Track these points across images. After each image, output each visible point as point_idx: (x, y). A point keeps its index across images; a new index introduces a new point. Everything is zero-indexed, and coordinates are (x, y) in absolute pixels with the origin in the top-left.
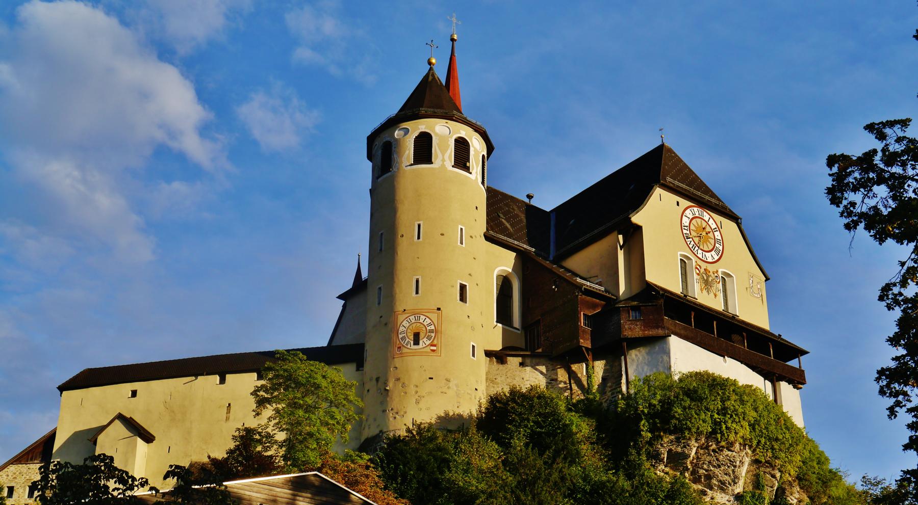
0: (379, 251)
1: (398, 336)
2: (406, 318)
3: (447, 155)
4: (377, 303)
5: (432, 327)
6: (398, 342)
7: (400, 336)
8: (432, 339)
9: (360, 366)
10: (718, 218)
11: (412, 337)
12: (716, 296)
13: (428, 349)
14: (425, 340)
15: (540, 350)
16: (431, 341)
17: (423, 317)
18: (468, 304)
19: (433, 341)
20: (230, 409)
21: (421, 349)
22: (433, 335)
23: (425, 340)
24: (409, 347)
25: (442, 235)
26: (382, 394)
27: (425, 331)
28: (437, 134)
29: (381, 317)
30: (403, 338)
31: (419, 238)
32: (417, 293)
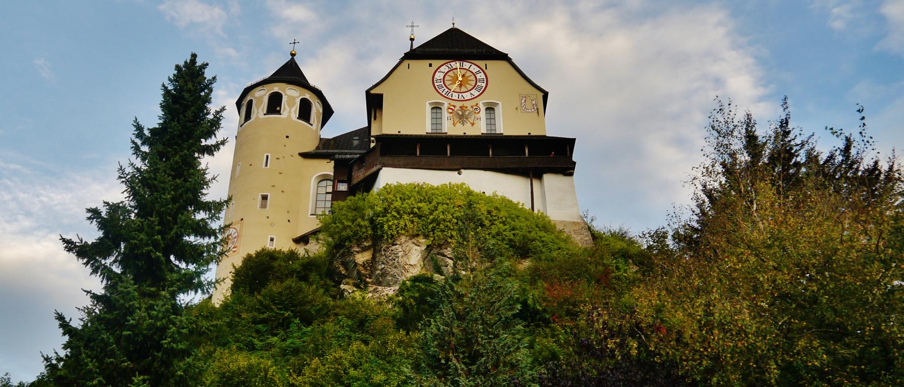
10: (482, 63)
12: (473, 124)
18: (268, 209)
22: (236, 240)
25: (251, 165)
28: (255, 98)
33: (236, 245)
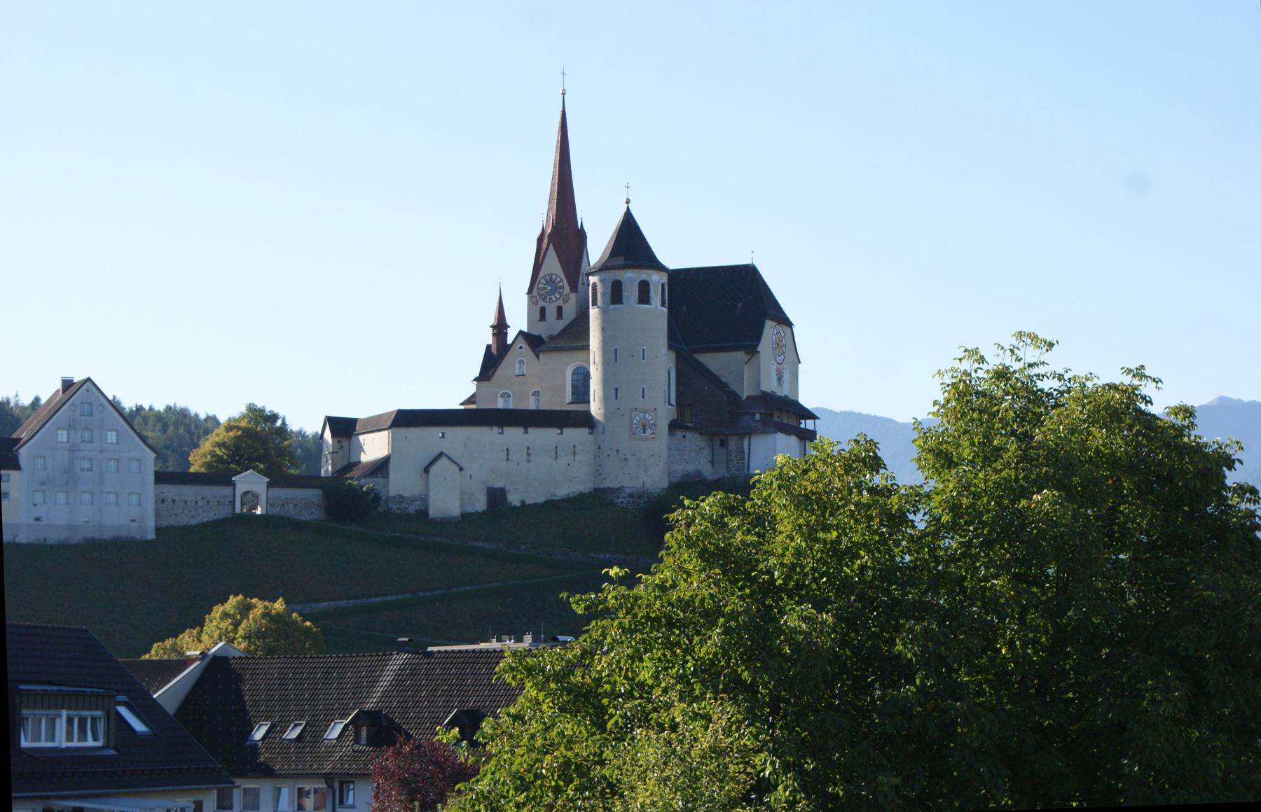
1: (632, 425)
3: (658, 298)
5: (652, 422)
11: (642, 428)
17: (647, 415)
22: (653, 427)
30: (636, 428)
31: (643, 359)
32: (643, 397)
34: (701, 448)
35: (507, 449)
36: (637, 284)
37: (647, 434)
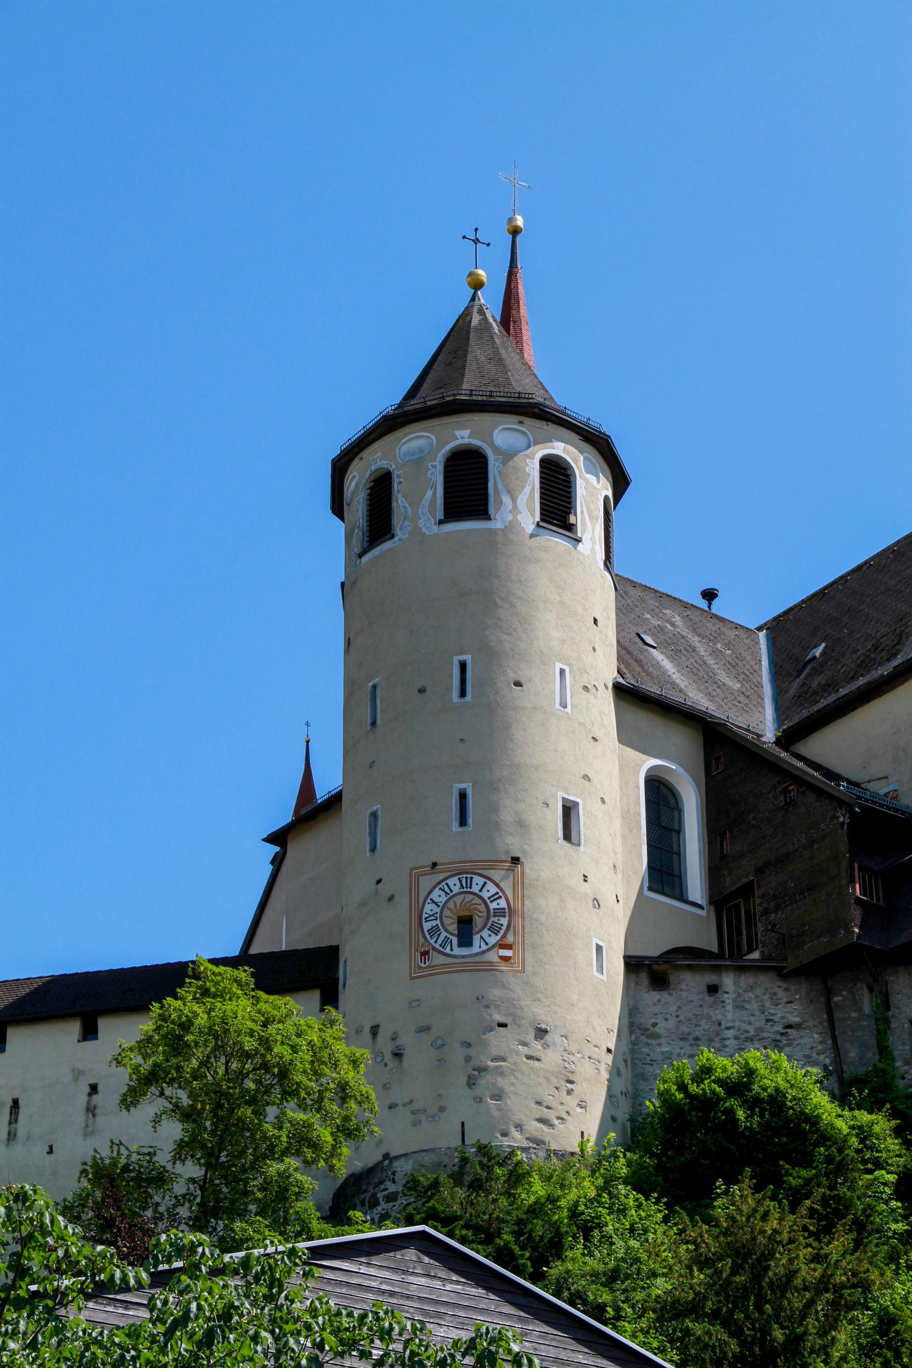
0: (369, 727)
2: (440, 883)
3: (522, 500)
4: (368, 849)
5: (503, 903)
6: (422, 940)
7: (427, 926)
8: (502, 932)
9: (330, 997)
11: (453, 928)
13: (493, 956)
14: (485, 933)
15: (756, 955)
16: (500, 935)
19: (504, 936)
20: (17, 1113)
21: (477, 954)
22: (504, 921)
23: (485, 933)
24: (448, 950)
25: (518, 684)
26: (386, 1065)
27: (485, 914)
28: (497, 450)
29: (379, 881)
30: (434, 931)
31: (463, 693)
32: (463, 822)
33: (510, 939)
34: (789, 1027)
35: (16, 1102)
36: (440, 468)
37: (475, 949)
